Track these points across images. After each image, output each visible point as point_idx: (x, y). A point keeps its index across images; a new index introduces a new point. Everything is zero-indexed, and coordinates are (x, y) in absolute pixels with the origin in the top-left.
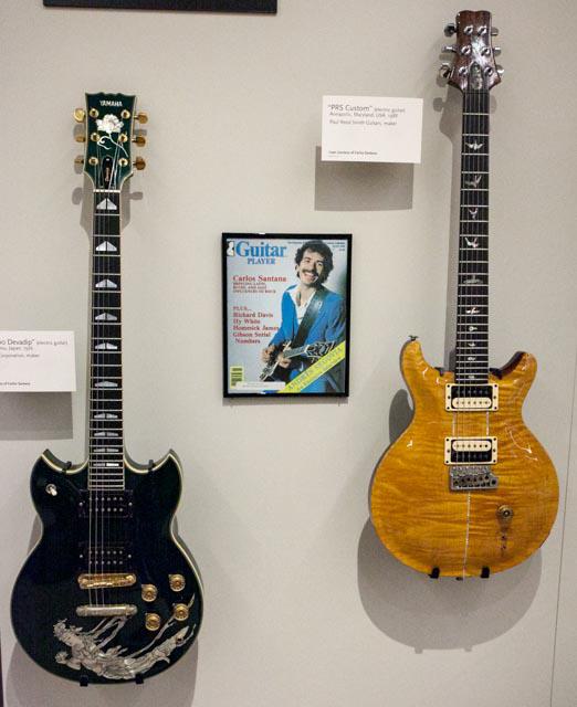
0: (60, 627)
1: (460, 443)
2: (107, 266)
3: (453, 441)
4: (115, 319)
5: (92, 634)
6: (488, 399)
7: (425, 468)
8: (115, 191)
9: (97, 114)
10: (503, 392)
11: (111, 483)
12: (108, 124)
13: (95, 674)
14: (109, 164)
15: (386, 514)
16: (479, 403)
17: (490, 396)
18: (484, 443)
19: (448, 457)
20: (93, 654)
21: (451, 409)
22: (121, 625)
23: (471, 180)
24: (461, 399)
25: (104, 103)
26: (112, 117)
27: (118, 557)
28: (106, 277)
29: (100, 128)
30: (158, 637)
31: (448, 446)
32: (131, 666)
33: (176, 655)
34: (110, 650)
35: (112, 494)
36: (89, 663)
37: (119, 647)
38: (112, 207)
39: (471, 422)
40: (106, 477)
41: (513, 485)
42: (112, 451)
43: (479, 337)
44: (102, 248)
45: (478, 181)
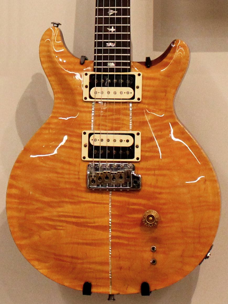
1: (97, 136)
3: (90, 135)
6: (130, 89)
7: (60, 165)
10: (148, 82)
15: (22, 214)
16: (123, 93)
18: (125, 138)
19: (85, 152)
21: (88, 99)
39: (112, 115)
41: (161, 188)
43: (119, 21)
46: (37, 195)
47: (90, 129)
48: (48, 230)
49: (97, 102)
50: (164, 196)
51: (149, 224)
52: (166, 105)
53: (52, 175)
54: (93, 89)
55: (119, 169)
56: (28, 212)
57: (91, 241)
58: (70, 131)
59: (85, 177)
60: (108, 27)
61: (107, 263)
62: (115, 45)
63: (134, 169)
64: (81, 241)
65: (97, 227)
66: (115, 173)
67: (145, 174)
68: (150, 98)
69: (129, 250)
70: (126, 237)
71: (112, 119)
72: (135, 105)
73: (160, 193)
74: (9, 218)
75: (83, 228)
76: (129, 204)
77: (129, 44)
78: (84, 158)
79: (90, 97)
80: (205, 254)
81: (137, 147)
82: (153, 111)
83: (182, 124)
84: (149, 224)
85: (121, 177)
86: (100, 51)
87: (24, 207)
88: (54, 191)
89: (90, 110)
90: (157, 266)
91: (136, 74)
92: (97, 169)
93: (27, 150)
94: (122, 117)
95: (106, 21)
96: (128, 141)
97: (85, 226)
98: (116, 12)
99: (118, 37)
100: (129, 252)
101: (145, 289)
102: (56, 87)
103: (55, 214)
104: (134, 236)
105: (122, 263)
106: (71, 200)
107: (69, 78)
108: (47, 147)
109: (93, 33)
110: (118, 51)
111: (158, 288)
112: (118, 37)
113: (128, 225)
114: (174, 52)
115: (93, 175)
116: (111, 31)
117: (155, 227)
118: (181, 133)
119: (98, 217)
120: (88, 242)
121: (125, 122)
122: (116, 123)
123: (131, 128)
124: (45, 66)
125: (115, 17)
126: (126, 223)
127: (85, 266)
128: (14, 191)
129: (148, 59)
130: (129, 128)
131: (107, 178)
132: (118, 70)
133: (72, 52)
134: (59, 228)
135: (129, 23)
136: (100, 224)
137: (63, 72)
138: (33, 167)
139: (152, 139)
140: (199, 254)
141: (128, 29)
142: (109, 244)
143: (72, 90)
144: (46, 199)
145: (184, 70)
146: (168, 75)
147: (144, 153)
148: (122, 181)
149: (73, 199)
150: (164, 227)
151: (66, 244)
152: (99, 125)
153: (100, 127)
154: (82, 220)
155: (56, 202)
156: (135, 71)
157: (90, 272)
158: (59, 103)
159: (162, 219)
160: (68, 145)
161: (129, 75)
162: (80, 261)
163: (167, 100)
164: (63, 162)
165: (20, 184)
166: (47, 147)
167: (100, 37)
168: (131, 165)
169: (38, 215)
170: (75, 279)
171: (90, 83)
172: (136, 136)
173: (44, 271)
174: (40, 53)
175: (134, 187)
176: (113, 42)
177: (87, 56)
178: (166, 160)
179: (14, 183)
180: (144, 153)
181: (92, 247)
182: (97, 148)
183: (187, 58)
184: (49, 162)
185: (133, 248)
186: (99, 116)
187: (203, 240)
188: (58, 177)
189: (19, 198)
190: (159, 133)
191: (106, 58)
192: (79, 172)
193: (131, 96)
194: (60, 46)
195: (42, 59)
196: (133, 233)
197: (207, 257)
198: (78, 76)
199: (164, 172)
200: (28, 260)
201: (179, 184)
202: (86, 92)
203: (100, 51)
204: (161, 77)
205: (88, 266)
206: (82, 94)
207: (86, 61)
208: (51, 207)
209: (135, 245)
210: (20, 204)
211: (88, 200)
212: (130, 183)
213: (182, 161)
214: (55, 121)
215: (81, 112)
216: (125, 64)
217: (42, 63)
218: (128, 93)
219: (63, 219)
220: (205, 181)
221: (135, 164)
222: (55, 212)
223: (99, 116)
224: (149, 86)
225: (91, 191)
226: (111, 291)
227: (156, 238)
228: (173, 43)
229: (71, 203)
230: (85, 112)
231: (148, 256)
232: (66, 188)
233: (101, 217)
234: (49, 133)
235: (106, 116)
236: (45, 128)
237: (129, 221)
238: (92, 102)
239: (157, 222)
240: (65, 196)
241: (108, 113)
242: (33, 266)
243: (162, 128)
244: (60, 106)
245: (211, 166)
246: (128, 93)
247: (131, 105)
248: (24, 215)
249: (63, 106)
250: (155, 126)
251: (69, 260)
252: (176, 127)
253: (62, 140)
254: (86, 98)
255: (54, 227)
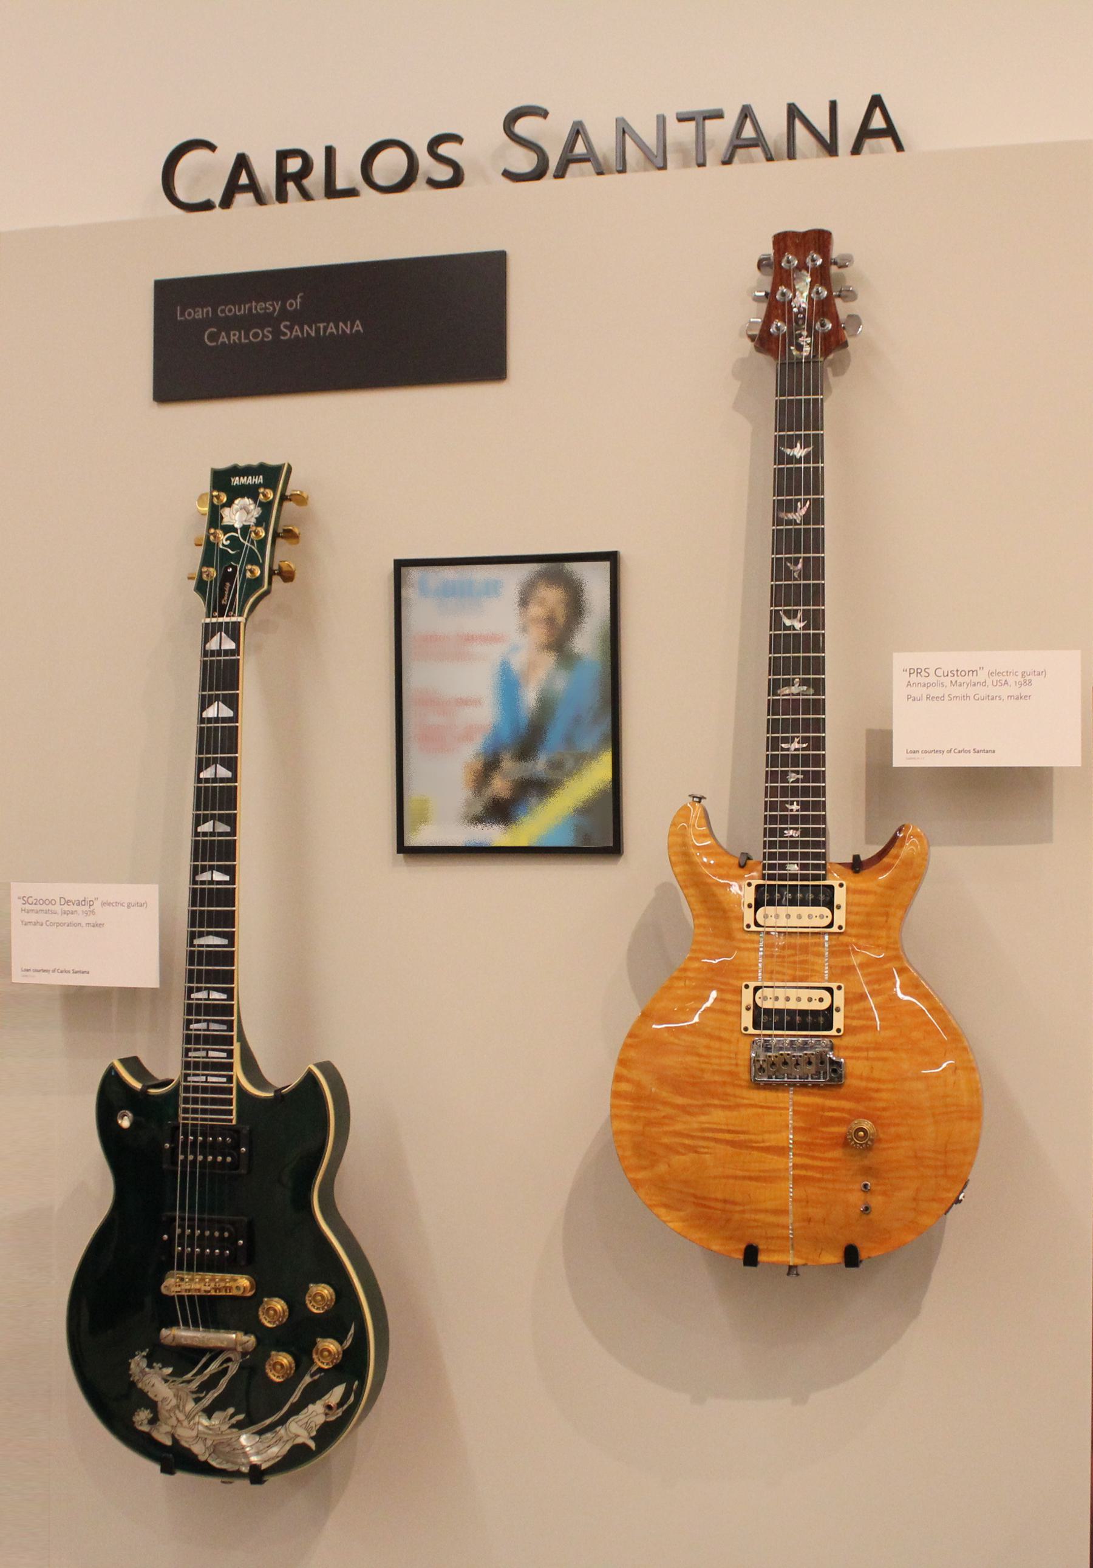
0: (138, 1363)
1: (768, 992)
2: (218, 742)
3: (756, 989)
4: (228, 829)
5: (189, 1382)
6: (826, 911)
7: (704, 1041)
8: (234, 619)
9: (224, 498)
10: (857, 898)
11: (213, 1112)
12: (239, 514)
13: (195, 1456)
14: (230, 578)
15: (639, 1127)
16: (813, 916)
17: (830, 904)
19: (747, 1019)
20: (189, 1417)
21: (753, 928)
22: (233, 1368)
23: (789, 511)
24: (770, 910)
25: (236, 481)
26: (247, 501)
27: (222, 1243)
28: (215, 761)
29: (226, 521)
30: (294, 1398)
31: (747, 997)
32: (253, 1448)
33: (328, 1434)
34: (217, 1414)
35: (213, 1130)
36: (186, 1436)
37: (231, 1410)
38: (229, 645)
39: (794, 955)
40: (205, 1101)
41: (879, 1081)
42: (216, 1055)
43: (805, 791)
44: (211, 712)
45: (803, 512)
46: (664, 1094)
47: (756, 979)
48: (683, 1154)
49: (768, 933)
50: (884, 1095)
51: (859, 1144)
52: (889, 937)
53: (689, 1059)
54: (761, 910)
55: (806, 1049)
56: (649, 1123)
57: (757, 1174)
58: (722, 983)
59: (747, 1063)
60: (787, 802)
61: (785, 1212)
62: (799, 833)
63: (832, 1048)
64: (740, 1173)
65: (768, 1150)
66: (800, 1055)
67: (851, 1058)
68: (861, 925)
69: (823, 1188)
70: (818, 1167)
71: (795, 962)
72: (834, 937)
73: (877, 1091)
74: (616, 1133)
75: (745, 1151)
76: (823, 1108)
77: (823, 832)
78: (746, 1029)
79: (757, 924)
80: (956, 1195)
81: (838, 1010)
82: (866, 949)
83: (916, 971)
84: (859, 1144)
85: (810, 1063)
86: (772, 845)
87: (642, 1114)
88: (694, 1087)
89: (756, 946)
90: (871, 1216)
91: (835, 884)
92: (768, 1049)
93: (647, 1016)
94: (811, 958)
95: (784, 791)
96: (821, 1000)
97: (747, 1147)
98: (800, 776)
99: (805, 819)
100: (824, 1191)
101: (851, 1257)
102: (698, 907)
103: (696, 1126)
104: (832, 1164)
105: (811, 1211)
106: (723, 1103)
107: (719, 891)
108: (682, 1010)
109: (762, 813)
110: (805, 845)
111: (873, 1255)
112: (805, 819)
113: (821, 1145)
114: (902, 846)
115: (761, 1058)
116: (792, 810)
117: (869, 1148)
118: (914, 987)
119: (770, 1132)
120: (753, 1174)
121: (816, 967)
122: (801, 970)
123: (826, 977)
124: (678, 869)
125: (800, 784)
126: (818, 1141)
127: (747, 1216)
128: (624, 1087)
129: (856, 858)
130: (823, 977)
131: (785, 1063)
132: (804, 878)
133: (725, 846)
134: (702, 1150)
135: (824, 796)
136: (773, 1143)
137: (709, 881)
138: (657, 1045)
139: (862, 997)
140: (945, 1195)
141: (822, 806)
142: (788, 1179)
143: (724, 911)
144: (680, 1101)
145: (918, 877)
146: (891, 886)
147: (849, 1022)
148: (811, 1069)
149: (727, 1100)
150: (884, 1149)
151: (715, 1177)
152: (772, 972)
153: (774, 976)
154: (742, 1137)
155: (696, 1106)
156: (835, 879)
157: (757, 1227)
158: (701, 935)
159: (881, 1136)
160: (718, 1006)
161: (824, 886)
162: (738, 1208)
163: (890, 928)
164: (711, 1036)
165: (635, 1074)
166: (682, 1010)
167: (773, 819)
168: (826, 1041)
169: (666, 1128)
170: (731, 1238)
171: (756, 900)
172: (835, 991)
173: (677, 1225)
174: (669, 847)
175: (831, 1079)
176: (796, 829)
177: (751, 854)
178: (888, 1033)
179: (625, 1072)
180: (849, 1022)
181: (759, 1184)
182: (768, 1012)
183: (925, 856)
184: (684, 1037)
185: (830, 1186)
186: (772, 956)
187: (951, 1172)
188: (700, 1063)
189: (633, 1100)
190: (876, 987)
191: (783, 856)
192: (736, 1054)
193: (827, 922)
194: (705, 836)
195: (673, 858)
196: (830, 1160)
197: (958, 1201)
198: (735, 888)
199: (885, 1054)
200: (650, 1206)
201: (909, 1074)
202: (748, 915)
203: (772, 845)
204: (879, 890)
205: (753, 1216)
206: (741, 918)
207: (749, 862)
208: (689, 1113)
209: (834, 1181)
210: (635, 1108)
211: (752, 1102)
212: (825, 1073)
213: (916, 1035)
214: (696, 965)
215: (740, 949)
216: (816, 867)
217: (673, 864)
218: (822, 917)
219: (710, 1135)
220: (954, 1069)
221: (833, 1040)
222: (694, 1123)
223: (772, 956)
224: (859, 905)
225: (757, 1086)
226: (792, 1260)
227: (870, 1168)
228: (900, 830)
229: (723, 1107)
230: (748, 949)
231: (856, 1198)
232: (715, 1082)
233: (775, 1132)
234: (685, 987)
235: (784, 957)
236: (678, 978)
237: (822, 1138)
238: (759, 932)
239: (872, 1140)
240: (713, 1095)
241: (788, 952)
242: (658, 1216)
243: (880, 978)
244: (704, 939)
245: (966, 1044)
246: (822, 917)
247: (827, 937)
248: (641, 1128)
249: (710, 939)
250: (869, 974)
251: (719, 1205)
252: (905, 975)
253: (707, 999)
254: (748, 926)
255: (694, 1150)
